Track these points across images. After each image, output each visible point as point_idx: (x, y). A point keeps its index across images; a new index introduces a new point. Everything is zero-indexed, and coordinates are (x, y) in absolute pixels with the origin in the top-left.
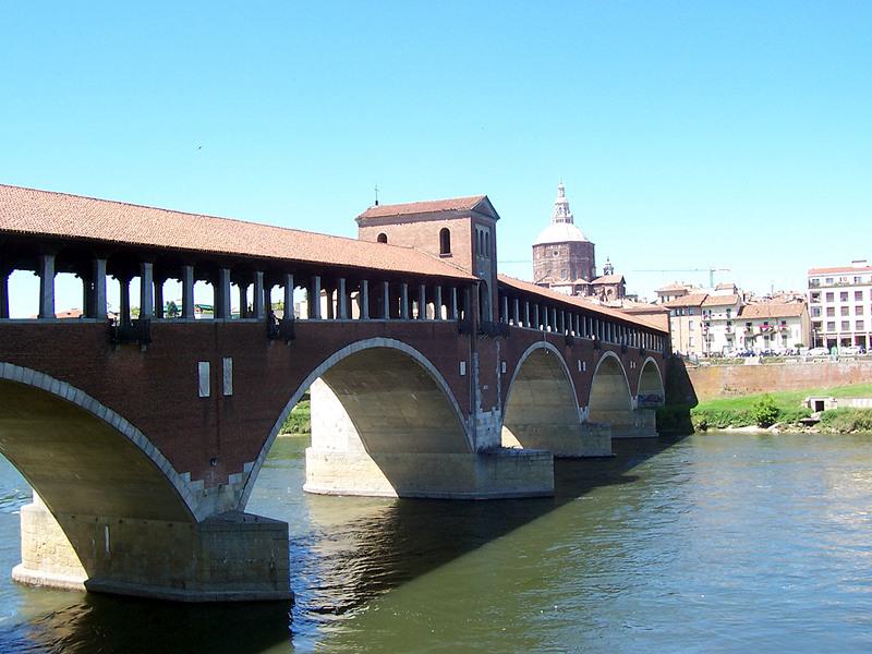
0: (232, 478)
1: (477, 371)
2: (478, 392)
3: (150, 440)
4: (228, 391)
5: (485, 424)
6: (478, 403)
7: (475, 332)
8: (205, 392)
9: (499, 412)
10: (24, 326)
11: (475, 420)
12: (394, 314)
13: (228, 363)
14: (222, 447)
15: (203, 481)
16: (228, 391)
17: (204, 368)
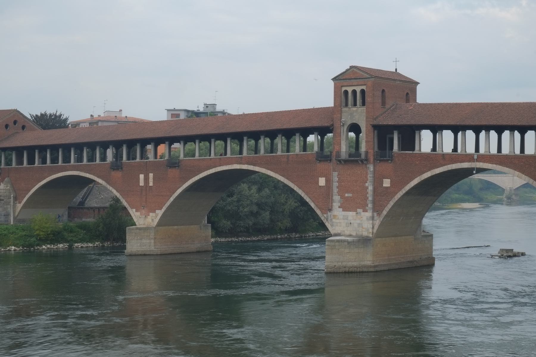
0: (151, 214)
1: (335, 184)
2: (336, 198)
3: (122, 197)
4: (151, 184)
5: (347, 219)
6: (336, 205)
7: (334, 159)
8: (142, 183)
9: (369, 214)
10: (426, 155)
11: (335, 216)
12: (142, 158)
13: (151, 175)
14: (147, 203)
15: (140, 213)
16: (151, 184)
17: (142, 176)
